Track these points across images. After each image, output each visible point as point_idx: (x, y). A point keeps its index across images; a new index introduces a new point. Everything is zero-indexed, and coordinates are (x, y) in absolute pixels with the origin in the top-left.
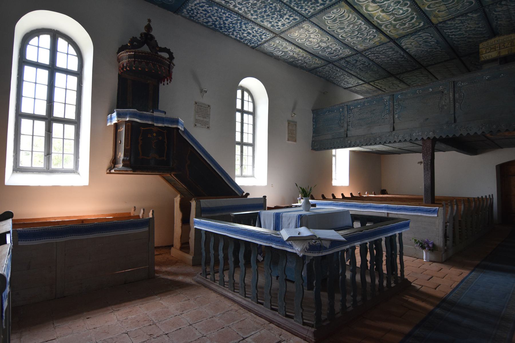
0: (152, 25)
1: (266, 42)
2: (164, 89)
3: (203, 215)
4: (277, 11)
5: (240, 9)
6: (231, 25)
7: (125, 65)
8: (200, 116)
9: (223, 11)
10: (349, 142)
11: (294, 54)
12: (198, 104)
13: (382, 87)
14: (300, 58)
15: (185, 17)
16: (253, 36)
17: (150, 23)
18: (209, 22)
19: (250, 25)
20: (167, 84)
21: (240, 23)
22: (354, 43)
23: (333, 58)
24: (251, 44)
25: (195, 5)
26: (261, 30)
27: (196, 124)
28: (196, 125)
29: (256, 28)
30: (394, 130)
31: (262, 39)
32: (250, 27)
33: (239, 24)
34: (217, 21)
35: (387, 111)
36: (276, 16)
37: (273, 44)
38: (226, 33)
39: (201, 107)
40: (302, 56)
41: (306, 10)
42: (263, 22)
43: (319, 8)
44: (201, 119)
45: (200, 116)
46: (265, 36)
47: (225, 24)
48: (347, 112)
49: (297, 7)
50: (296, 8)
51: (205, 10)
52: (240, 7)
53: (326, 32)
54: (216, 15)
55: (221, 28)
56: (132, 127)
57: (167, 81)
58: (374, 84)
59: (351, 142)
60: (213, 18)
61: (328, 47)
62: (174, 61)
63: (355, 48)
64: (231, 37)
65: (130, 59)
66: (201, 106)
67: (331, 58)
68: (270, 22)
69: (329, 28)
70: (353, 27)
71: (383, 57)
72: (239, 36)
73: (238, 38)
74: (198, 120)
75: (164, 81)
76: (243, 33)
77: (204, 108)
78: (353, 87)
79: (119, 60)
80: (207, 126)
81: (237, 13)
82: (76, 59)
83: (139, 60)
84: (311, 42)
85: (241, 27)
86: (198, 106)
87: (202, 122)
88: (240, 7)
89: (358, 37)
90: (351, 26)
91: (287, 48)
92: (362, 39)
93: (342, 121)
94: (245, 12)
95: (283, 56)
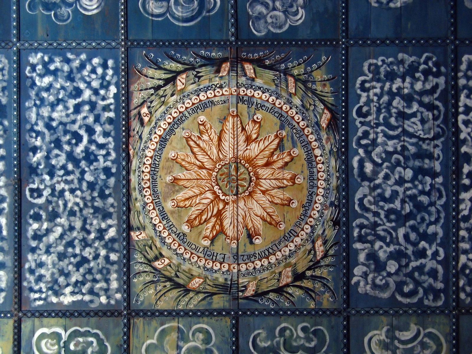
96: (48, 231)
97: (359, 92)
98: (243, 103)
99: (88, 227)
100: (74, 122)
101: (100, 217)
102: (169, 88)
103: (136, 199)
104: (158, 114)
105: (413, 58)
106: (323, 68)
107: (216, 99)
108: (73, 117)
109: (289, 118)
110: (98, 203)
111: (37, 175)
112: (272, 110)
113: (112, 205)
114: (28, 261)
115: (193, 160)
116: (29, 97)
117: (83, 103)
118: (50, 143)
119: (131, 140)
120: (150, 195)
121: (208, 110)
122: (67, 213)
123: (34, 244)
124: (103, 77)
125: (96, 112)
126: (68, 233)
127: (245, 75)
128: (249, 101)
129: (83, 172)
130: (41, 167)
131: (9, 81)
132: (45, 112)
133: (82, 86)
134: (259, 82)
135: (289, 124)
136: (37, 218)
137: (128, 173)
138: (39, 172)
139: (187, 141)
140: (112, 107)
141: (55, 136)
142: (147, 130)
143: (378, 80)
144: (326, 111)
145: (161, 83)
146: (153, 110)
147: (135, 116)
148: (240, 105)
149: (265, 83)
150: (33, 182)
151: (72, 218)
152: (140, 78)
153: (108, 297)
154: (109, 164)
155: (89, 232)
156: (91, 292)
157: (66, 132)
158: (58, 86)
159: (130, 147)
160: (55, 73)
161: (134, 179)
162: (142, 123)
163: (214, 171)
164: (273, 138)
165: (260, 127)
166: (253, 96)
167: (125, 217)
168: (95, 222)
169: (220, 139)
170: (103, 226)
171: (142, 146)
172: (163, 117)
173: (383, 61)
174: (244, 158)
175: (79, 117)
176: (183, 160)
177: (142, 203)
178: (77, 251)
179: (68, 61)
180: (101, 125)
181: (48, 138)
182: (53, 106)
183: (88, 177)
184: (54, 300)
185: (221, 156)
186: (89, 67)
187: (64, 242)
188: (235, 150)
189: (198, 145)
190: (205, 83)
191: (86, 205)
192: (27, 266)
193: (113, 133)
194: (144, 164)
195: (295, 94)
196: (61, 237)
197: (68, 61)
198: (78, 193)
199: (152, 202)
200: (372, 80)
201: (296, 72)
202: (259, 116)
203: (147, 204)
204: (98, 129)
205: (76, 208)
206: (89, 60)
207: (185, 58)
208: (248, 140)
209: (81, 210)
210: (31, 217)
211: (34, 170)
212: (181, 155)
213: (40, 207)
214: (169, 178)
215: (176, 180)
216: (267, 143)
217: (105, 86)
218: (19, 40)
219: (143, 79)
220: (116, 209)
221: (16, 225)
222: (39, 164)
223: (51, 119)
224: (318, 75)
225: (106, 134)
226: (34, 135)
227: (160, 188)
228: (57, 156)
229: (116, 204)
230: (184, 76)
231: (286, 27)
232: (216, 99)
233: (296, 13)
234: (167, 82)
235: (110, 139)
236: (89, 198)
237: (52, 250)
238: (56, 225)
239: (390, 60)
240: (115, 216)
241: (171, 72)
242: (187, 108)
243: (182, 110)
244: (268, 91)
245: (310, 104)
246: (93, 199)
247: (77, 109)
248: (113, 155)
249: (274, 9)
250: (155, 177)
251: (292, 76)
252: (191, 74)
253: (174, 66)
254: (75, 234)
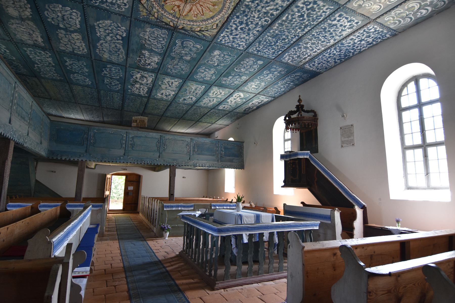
12: (342, 128)
27: (343, 145)
28: (342, 146)
44: (346, 139)
45: (345, 138)
66: (345, 129)
77: (348, 129)
80: (352, 144)
86: (343, 129)
96: (272, 10)
97: (127, 4)
98: (177, 17)
99: (256, 5)
100: (240, 33)
101: (250, 6)
102: (203, 29)
103: (232, 6)
104: (210, 25)
105: (102, 5)
106: (142, 15)
107: (187, 21)
108: (240, 34)
109: (159, 7)
110: (247, 10)
111: (262, 25)
112: (166, 11)
113: (243, 8)
114: (287, 4)
115: (204, 9)
116: (249, 42)
117: (233, 35)
118: (251, 31)
119: (224, 22)
120: (226, 5)
121: (191, 19)
122: (261, 12)
123: (280, 8)
124: (223, 38)
125: (231, 32)
126: (265, 6)
127: (173, 23)
128: (174, 16)
129: (246, 20)
130: (259, 26)
131: (253, 46)
132: (247, 38)
133: (231, 39)
134: (169, 20)
135: (160, 5)
136: (272, 15)
137: (230, 14)
138: (261, 26)
139: (203, 15)
140: (225, 31)
141: (248, 32)
142: (217, 22)
143: (118, 4)
144: (143, 3)
145: (205, 31)
146: (212, 26)
147: (218, 27)
148: (178, 17)
149: (166, 19)
150: (265, 24)
152: (212, 35)
154: (236, 19)
155: (257, 3)
157: (245, 31)
158: (239, 41)
159: (225, 20)
160: (238, 44)
161: (230, 12)
162: (217, 25)
163: (197, 3)
164: (168, 4)
165: (173, 9)
166: (172, 17)
167: (240, 3)
168: (253, 5)
169: (190, 11)
170: (250, 3)
171: (221, 19)
172: (209, 24)
173: (116, 9)
174: (183, 2)
175: (237, 33)
176: (208, 10)
177: (231, 4)
179: (232, 45)
180: (231, 29)
181: (251, 32)
182: (244, 38)
183: (245, 18)
185: (192, 6)
186: (226, 42)
187: (268, 4)
188: (185, 6)
189: (199, 12)
190: (190, 26)
191: (252, 11)
192: (288, 3)
193: (229, 26)
194: (223, 14)
195: (155, 12)
196: (268, 6)
197: (232, 45)
198: (252, 16)
199: (227, 3)
200: (121, 5)
201: (153, 18)
202: (172, 12)
203: (229, 3)
204: (233, 28)
205: (256, 12)
206: (225, 43)
207: (194, 34)
208: (179, 7)
209: (255, 11)
210: (274, 16)
211: (262, 26)
212: (208, 12)
213: (268, 17)
214: (216, 7)
215: (214, 6)
216: (171, 3)
217: (224, 37)
218: (242, 53)
219: (211, 34)
220: (242, 6)
221: (281, 16)
222: (259, 27)
223: (247, 36)
224: (144, 14)
225: (232, 26)
226: (255, 34)
227: (221, 6)
228: (252, 27)
229: (241, 7)
230: (196, 30)
231: (154, 29)
232: (187, 21)
233: (149, 31)
234: (203, 31)
235: (231, 25)
236: (250, 13)
237: (275, 4)
238: (267, 10)
239: (113, 8)
240: (244, 4)
241: (200, 33)
242: (199, 23)
243: (201, 23)
244: (166, 17)
245: (149, 7)
246: (248, 12)
247: (237, 35)
248: (232, 21)
249: (158, 34)
250: (221, 9)
251: (155, 17)
252: (193, 30)
253: (198, 33)
254: (263, 5)
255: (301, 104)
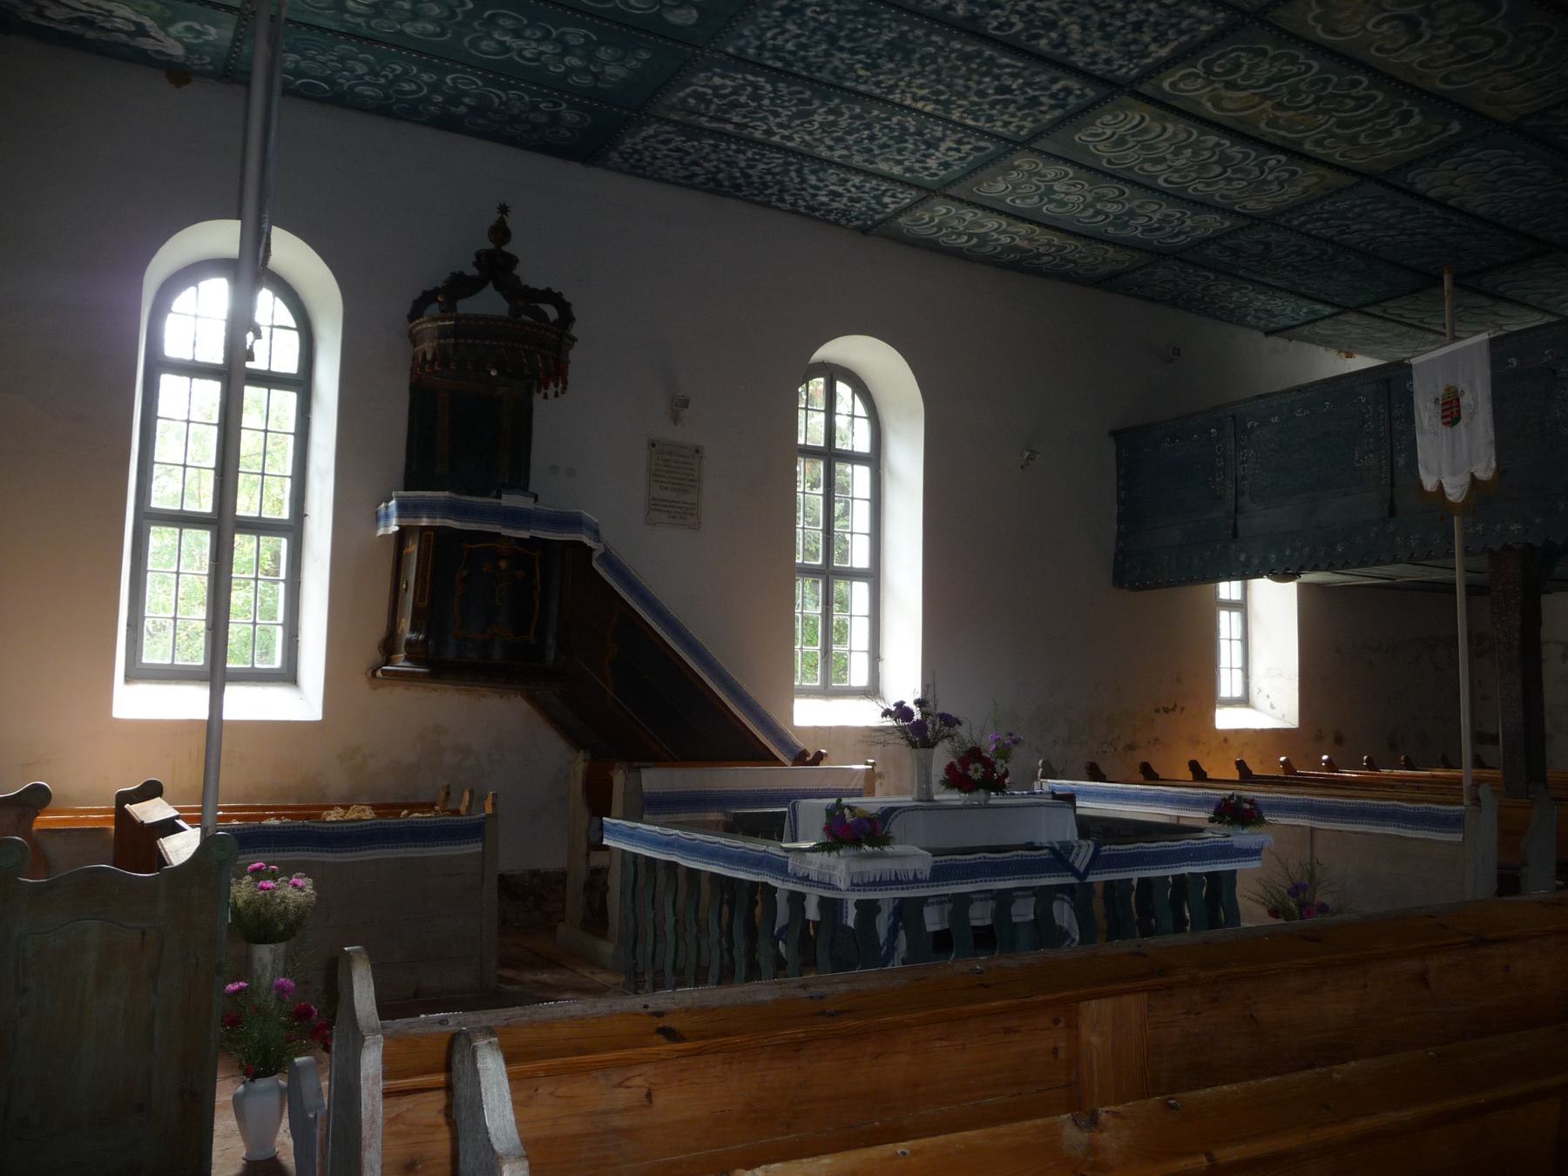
0: (511, 222)
1: (899, 213)
2: (547, 411)
3: (646, 817)
4: (911, 135)
5: (790, 138)
6: (769, 178)
7: (429, 357)
8: (666, 485)
9: (733, 147)
10: (1242, 557)
11: (1013, 239)
13: (1425, 320)
14: (1041, 250)
15: (618, 170)
16: (851, 200)
17: (505, 216)
18: (695, 175)
19: (832, 175)
20: (556, 395)
21: (799, 172)
22: (1222, 196)
23: (1169, 241)
24: (849, 221)
25: (644, 139)
26: (874, 182)
29: (857, 180)
30: (1392, 512)
31: (885, 206)
32: (834, 179)
33: (793, 174)
34: (719, 170)
35: (1371, 440)
36: (911, 146)
37: (927, 217)
38: (758, 199)
39: (668, 457)
40: (1049, 244)
41: (1006, 124)
42: (872, 163)
43: (1048, 117)
45: (666, 488)
46: (893, 196)
47: (750, 176)
48: (1236, 442)
49: (976, 119)
50: (969, 122)
51: (678, 150)
52: (786, 133)
53: (1105, 174)
54: (713, 156)
55: (738, 187)
56: (440, 547)
57: (556, 386)
58: (1384, 311)
59: (1249, 559)
60: (706, 165)
61: (1131, 214)
62: (575, 331)
63: (1236, 208)
64: (778, 208)
65: (442, 341)
67: (1159, 242)
68: (899, 163)
69: (1109, 162)
70: (1195, 154)
71: (1367, 226)
72: (801, 202)
73: (802, 209)
74: (657, 502)
75: (546, 388)
76: (815, 196)
78: (1299, 325)
79: (414, 339)
81: (779, 148)
82: (294, 337)
83: (470, 341)
84: (1062, 204)
85: (803, 181)
87: (673, 507)
88: (786, 133)
89: (1229, 180)
90: (1188, 152)
91: (983, 226)
92: (1249, 184)
93: (1219, 477)
94: (807, 144)
95: (974, 246)
151: (1075, 12)
153: (1209, 24)
156: (1181, 33)
178: (1119, 23)
184: (1149, 60)
187: (1093, 29)
210: (1028, 40)
255: (505, 248)
